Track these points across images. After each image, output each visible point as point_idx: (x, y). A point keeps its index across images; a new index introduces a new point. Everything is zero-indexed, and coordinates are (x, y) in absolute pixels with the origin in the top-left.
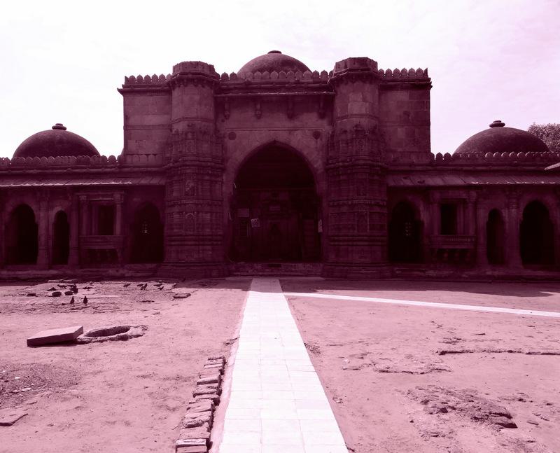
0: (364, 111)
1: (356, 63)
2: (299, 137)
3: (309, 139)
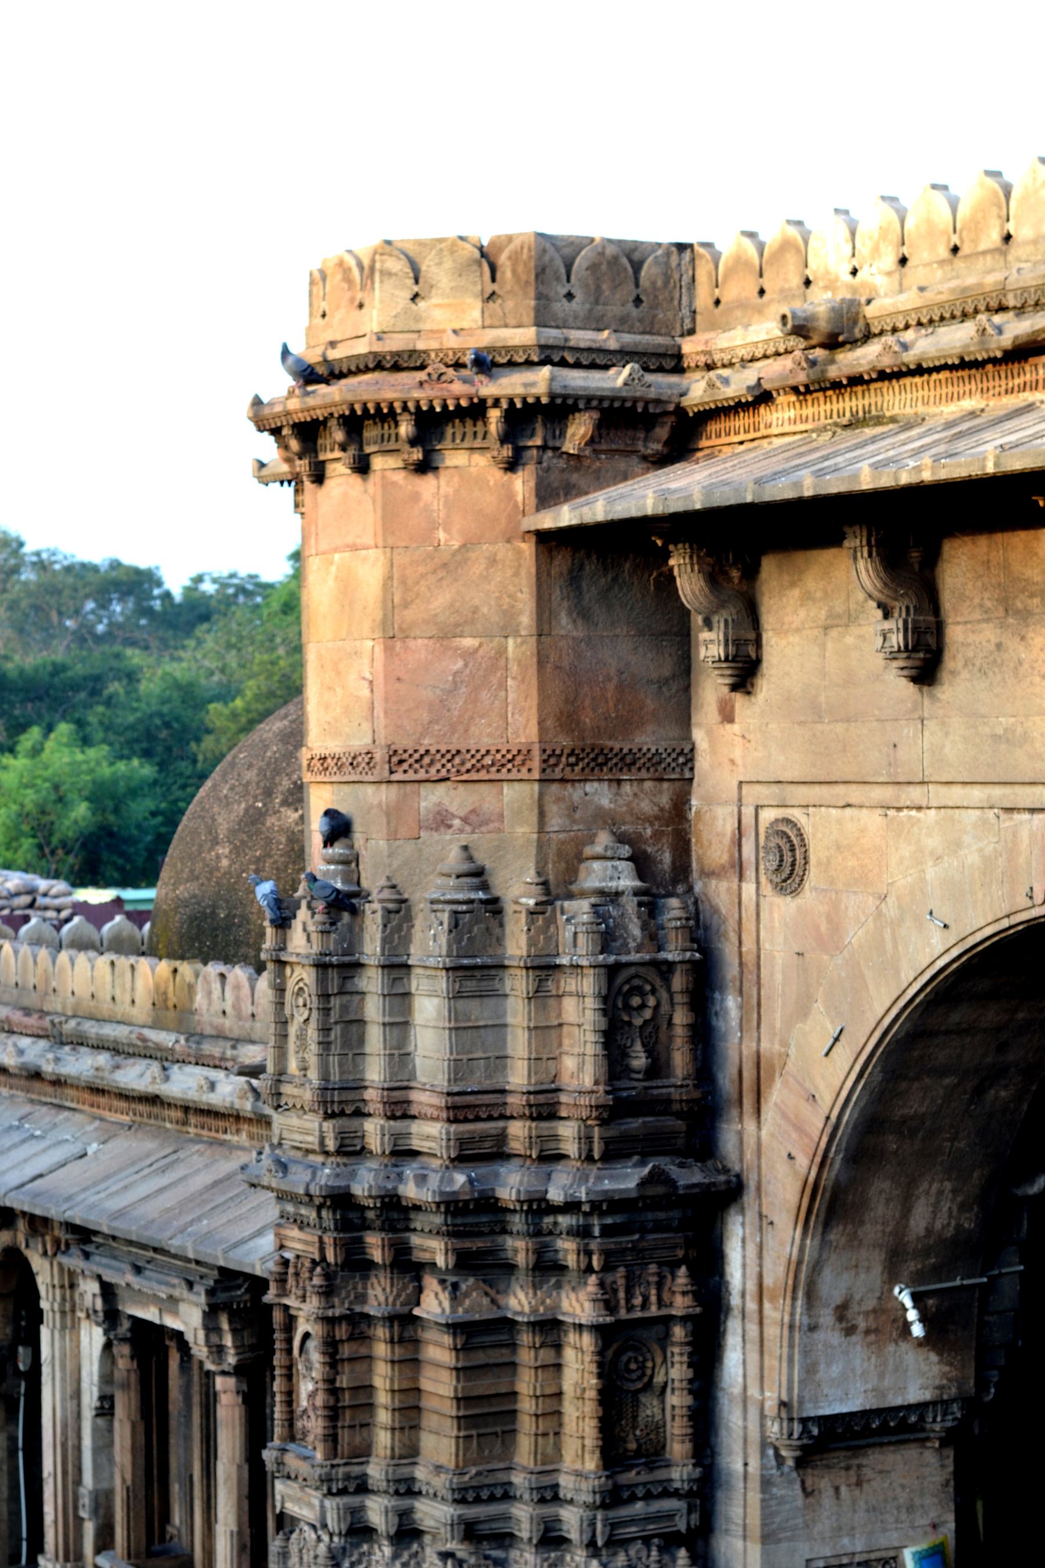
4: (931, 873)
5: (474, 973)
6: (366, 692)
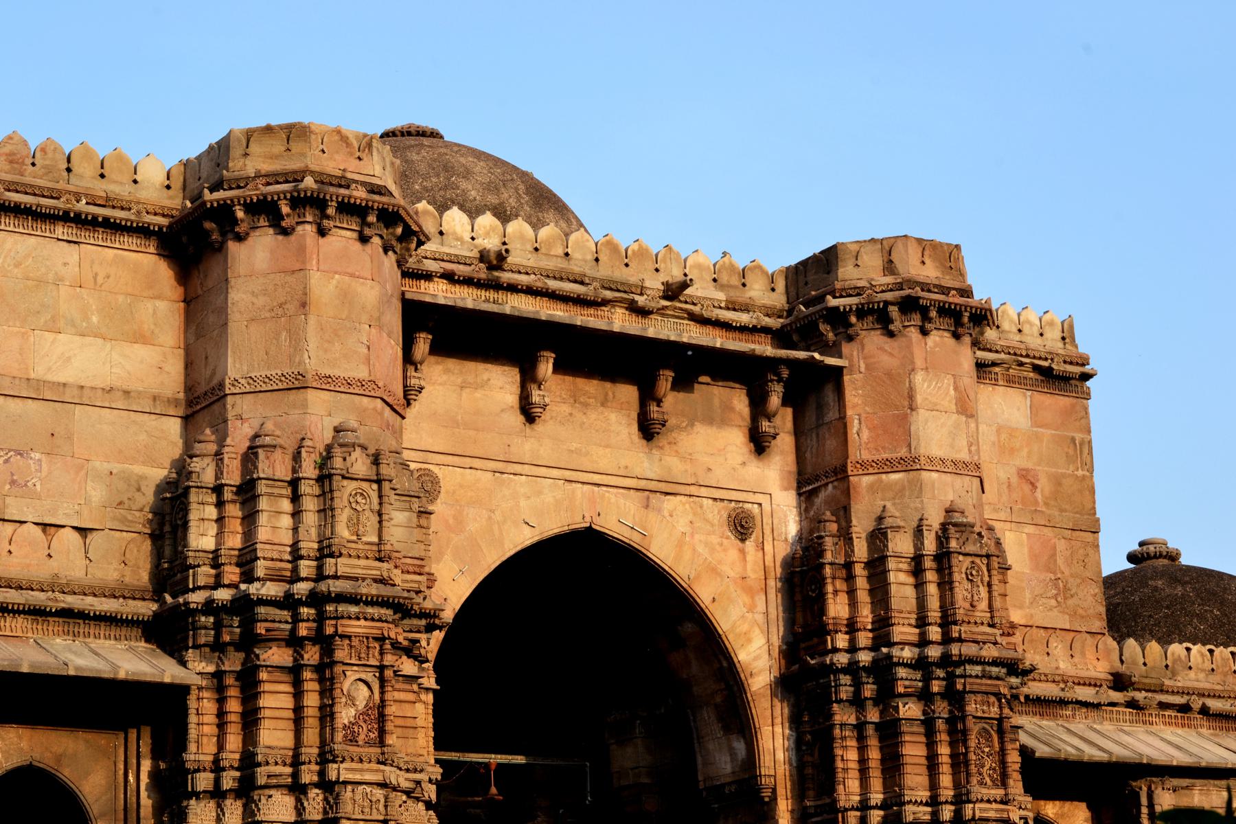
2: (682, 525)
3: (715, 539)
4: (523, 503)
6: (366, 351)
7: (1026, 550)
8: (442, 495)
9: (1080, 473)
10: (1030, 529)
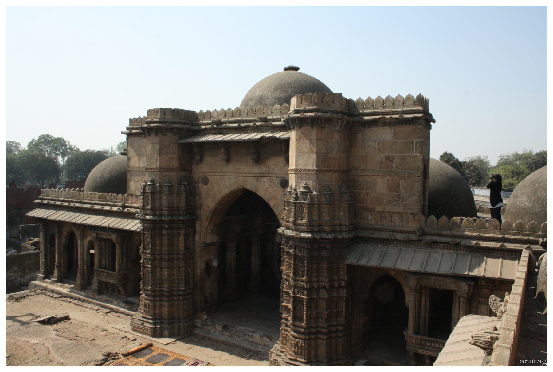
0: (310, 167)
1: (303, 102)
2: (267, 185)
3: (276, 188)
4: (227, 183)
5: (170, 193)
7: (386, 185)
8: (209, 183)
9: (415, 154)
10: (389, 178)
